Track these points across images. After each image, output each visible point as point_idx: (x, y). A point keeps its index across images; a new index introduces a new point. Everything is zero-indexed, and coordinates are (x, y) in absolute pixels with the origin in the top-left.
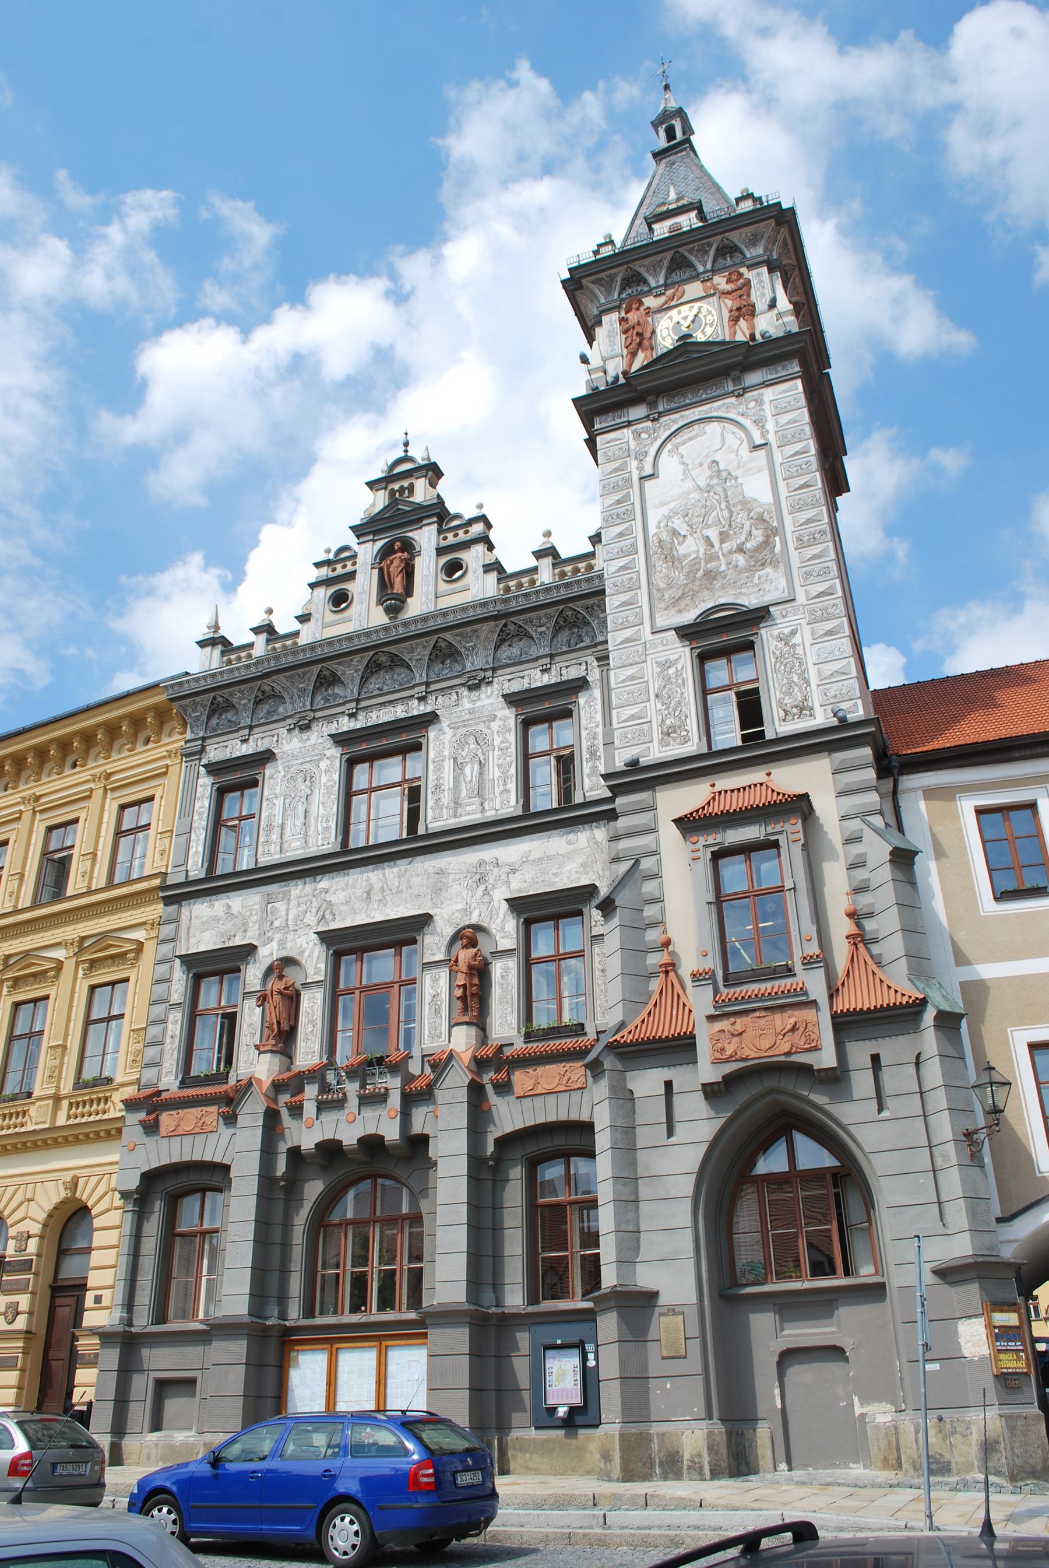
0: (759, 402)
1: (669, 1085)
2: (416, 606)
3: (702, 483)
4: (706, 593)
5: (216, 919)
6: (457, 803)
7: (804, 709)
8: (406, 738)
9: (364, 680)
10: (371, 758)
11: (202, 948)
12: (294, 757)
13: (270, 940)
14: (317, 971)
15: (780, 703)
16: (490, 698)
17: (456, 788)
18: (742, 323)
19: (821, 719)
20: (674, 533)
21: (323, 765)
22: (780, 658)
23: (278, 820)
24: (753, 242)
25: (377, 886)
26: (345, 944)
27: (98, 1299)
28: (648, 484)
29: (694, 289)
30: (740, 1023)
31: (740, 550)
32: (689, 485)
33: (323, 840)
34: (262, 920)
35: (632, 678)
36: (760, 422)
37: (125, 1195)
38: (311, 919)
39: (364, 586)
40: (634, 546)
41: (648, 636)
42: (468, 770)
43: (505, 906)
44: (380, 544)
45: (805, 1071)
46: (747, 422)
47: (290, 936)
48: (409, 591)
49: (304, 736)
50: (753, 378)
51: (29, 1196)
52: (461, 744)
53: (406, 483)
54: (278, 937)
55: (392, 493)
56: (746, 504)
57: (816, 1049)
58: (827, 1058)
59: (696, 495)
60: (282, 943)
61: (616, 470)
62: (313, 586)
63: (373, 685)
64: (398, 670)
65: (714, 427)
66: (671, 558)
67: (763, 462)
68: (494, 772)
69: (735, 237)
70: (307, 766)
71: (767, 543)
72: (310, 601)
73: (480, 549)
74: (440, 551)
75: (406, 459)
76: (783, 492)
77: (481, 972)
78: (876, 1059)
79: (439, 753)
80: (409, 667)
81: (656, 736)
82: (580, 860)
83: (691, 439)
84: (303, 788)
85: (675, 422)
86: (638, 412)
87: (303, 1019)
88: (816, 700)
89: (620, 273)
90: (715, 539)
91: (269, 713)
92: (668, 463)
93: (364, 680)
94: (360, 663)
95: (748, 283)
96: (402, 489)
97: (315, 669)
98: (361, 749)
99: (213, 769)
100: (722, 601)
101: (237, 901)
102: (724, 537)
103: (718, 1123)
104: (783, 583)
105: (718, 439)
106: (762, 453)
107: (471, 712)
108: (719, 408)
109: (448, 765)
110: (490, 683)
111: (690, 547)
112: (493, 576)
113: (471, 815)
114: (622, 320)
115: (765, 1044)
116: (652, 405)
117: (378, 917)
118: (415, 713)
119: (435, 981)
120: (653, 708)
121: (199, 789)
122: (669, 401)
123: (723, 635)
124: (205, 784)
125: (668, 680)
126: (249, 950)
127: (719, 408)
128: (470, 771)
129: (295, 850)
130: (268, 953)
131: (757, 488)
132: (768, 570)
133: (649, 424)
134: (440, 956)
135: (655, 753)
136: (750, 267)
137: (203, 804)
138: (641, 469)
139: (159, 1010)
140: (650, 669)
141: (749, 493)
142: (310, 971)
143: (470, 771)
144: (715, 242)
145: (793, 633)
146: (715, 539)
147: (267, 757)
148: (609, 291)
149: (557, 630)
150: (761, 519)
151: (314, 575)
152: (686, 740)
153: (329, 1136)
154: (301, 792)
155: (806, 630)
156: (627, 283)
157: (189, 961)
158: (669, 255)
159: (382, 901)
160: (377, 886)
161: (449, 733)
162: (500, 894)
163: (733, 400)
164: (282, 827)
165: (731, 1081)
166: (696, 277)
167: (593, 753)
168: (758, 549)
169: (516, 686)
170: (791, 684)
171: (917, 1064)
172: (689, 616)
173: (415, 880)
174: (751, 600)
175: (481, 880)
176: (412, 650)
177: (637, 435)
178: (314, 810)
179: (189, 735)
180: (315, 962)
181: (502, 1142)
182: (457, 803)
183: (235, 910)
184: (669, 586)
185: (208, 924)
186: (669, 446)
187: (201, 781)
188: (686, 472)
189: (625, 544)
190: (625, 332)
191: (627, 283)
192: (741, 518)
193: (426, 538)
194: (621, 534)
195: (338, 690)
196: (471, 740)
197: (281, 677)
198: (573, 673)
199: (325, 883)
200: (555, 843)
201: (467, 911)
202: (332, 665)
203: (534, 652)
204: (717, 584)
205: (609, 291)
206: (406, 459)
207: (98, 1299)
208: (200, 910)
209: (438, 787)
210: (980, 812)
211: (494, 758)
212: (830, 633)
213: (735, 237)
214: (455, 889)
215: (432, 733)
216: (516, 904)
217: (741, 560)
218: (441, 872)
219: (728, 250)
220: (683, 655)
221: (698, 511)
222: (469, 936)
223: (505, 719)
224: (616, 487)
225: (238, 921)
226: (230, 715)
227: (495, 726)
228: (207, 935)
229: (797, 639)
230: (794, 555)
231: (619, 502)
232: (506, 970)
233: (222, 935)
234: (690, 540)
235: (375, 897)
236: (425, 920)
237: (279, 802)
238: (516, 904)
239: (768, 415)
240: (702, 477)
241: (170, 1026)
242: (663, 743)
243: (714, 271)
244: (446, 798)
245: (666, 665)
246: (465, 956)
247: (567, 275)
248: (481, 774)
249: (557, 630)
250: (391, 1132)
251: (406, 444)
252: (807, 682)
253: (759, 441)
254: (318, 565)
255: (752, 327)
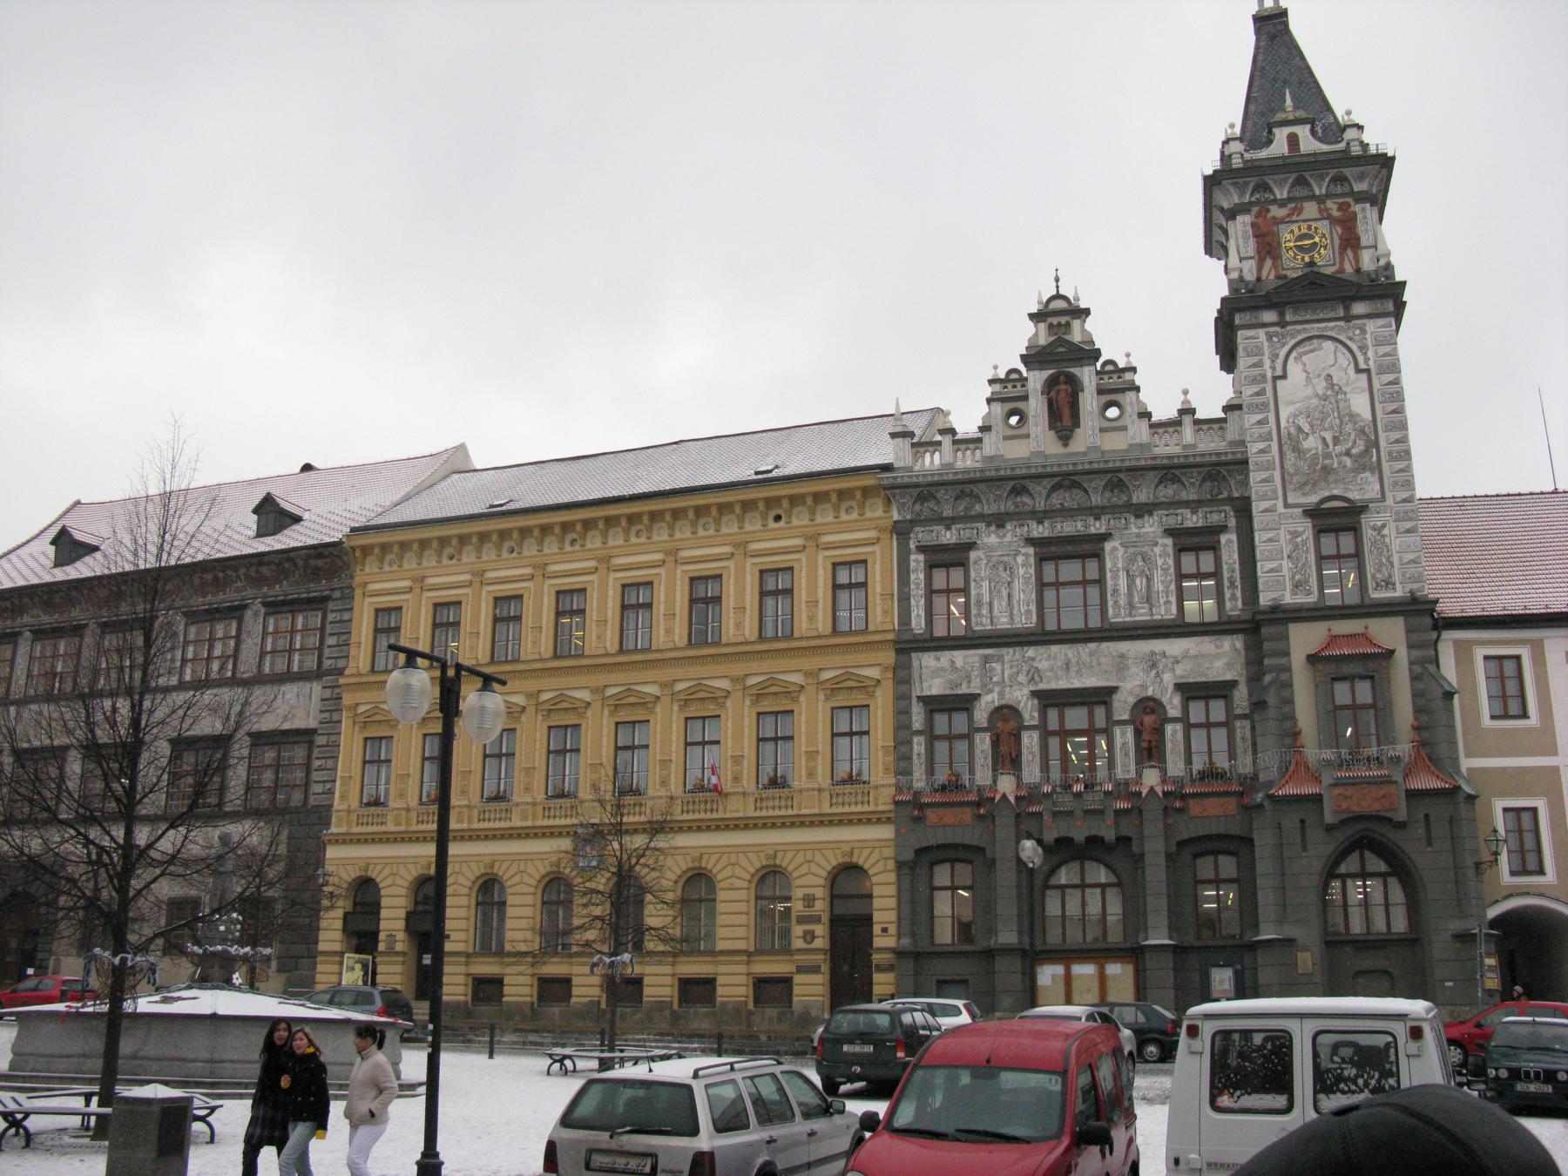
0: (1363, 331)
1: (1302, 821)
2: (1087, 438)
3: (1320, 392)
4: (1323, 484)
5: (942, 669)
6: (1131, 606)
7: (1389, 583)
8: (1090, 548)
9: (1048, 496)
10: (1056, 558)
11: (934, 692)
12: (991, 549)
13: (991, 691)
14: (1032, 718)
15: (1373, 577)
16: (1151, 526)
17: (1130, 595)
18: (1350, 253)
19: (1399, 592)
20: (1300, 429)
21: (1020, 559)
22: (1374, 544)
23: (986, 598)
24: (1361, 178)
25: (1074, 660)
26: (1049, 699)
27: (885, 930)
28: (1279, 383)
29: (1311, 209)
30: (1349, 791)
31: (1348, 453)
32: (1309, 391)
33: (1025, 619)
34: (982, 676)
35: (1270, 540)
36: (1363, 348)
37: (900, 865)
38: (1022, 678)
39: (1036, 406)
40: (1270, 433)
41: (1281, 509)
42: (1138, 582)
43: (1171, 688)
44: (1047, 373)
45: (1390, 820)
46: (1354, 347)
47: (1007, 690)
48: (1077, 424)
49: (1001, 532)
50: (1359, 308)
51: (809, 858)
52: (1132, 560)
53: (1063, 320)
54: (997, 689)
55: (1051, 326)
56: (1353, 417)
57: (1395, 810)
58: (1401, 815)
59: (1315, 401)
60: (1001, 694)
61: (1254, 365)
62: (989, 401)
63: (1056, 500)
64: (1075, 491)
65: (1328, 345)
66: (1298, 450)
67: (1365, 384)
68: (1158, 587)
69: (1347, 172)
70: (1006, 559)
71: (1367, 451)
72: (989, 414)
73: (1132, 394)
74: (1100, 392)
75: (1058, 296)
76: (1379, 415)
77: (1159, 731)
78: (1426, 816)
79: (1115, 564)
80: (1085, 491)
81: (1289, 587)
82: (1225, 660)
83: (1312, 351)
84: (1005, 575)
85: (1299, 332)
86: (1269, 316)
87: (1024, 751)
88: (1397, 578)
89: (1253, 182)
90: (1329, 441)
91: (966, 509)
92: (1294, 368)
93: (1048, 496)
94: (1048, 483)
95: (1354, 216)
96: (1059, 324)
97: (1012, 483)
98: (1048, 551)
99: (921, 549)
100: (1335, 492)
101: (959, 656)
102: (1336, 441)
103: (1332, 848)
104: (1378, 487)
105: (1332, 356)
106: (1364, 376)
107: (1138, 535)
108: (1332, 329)
109: (1122, 577)
110: (1151, 514)
111: (1311, 443)
112: (1144, 424)
113: (1142, 615)
114: (1253, 225)
115: (1365, 804)
116: (1282, 314)
117: (1077, 684)
118: (1093, 530)
119: (1123, 734)
120: (1286, 565)
121: (913, 564)
122: (1295, 313)
123: (1337, 521)
124: (917, 560)
125: (1297, 546)
126: (976, 697)
127: (1332, 329)
128: (1140, 583)
129: (1003, 623)
130: (989, 700)
131: (1360, 404)
132: (1368, 474)
133: (1277, 329)
134: (1126, 717)
135: (1288, 599)
136: (1357, 201)
137: (918, 577)
138: (1274, 369)
139: (903, 734)
140: (1283, 536)
141: (1355, 409)
142: (1026, 716)
143: (1140, 583)
144: (1332, 172)
145: (1384, 526)
146: (1329, 441)
147: (971, 546)
148: (1242, 194)
149: (1204, 480)
150: (1362, 431)
151: (988, 391)
152: (1309, 593)
153: (1063, 833)
154: (1003, 582)
155: (1392, 525)
156: (1256, 189)
157: (926, 700)
158: (1294, 176)
159: (1078, 671)
160: (1074, 660)
161: (1122, 551)
162: (1169, 679)
163: (1342, 323)
164: (991, 604)
165: (1343, 822)
166: (1313, 197)
167: (1232, 583)
168: (1361, 455)
169: (1172, 522)
170: (1381, 564)
171: (1451, 821)
172: (1313, 499)
173: (1103, 660)
174: (1354, 495)
175: (1154, 666)
176: (1091, 481)
177: (1269, 337)
178: (1016, 594)
179: (896, 517)
180: (1030, 712)
181: (1181, 844)
182: (1131, 606)
183: (959, 663)
184: (1296, 473)
185: (938, 672)
186: (1294, 354)
187: (913, 557)
188: (1308, 379)
189: (1264, 430)
190: (1255, 236)
191: (1256, 189)
192: (1348, 427)
193: (1087, 376)
194: (1260, 422)
195: (1026, 499)
196: (1139, 558)
197: (983, 486)
198: (1215, 518)
199: (1031, 652)
200: (1205, 645)
201: (1144, 687)
202: (1027, 483)
203: (1184, 496)
204: (1331, 478)
205: (1242, 194)
206: (1058, 296)
207: (885, 930)
208: (927, 662)
209: (1115, 591)
210: (1486, 658)
211: (1158, 576)
212: (1408, 531)
213: (1347, 172)
214: (1134, 670)
215: (1108, 546)
216: (1179, 687)
217: (1348, 462)
218: (1122, 656)
219: (1340, 179)
220: (1306, 528)
221: (1317, 415)
222: (1148, 706)
223: (1165, 545)
224: (1254, 381)
225: (962, 674)
226: (932, 504)
227: (1157, 550)
228: (937, 681)
229: (1385, 531)
230: (1385, 465)
231: (1257, 394)
232: (1175, 732)
233: (950, 682)
234: (1311, 438)
235: (1073, 669)
236: (1112, 690)
237: (985, 584)
238: (1179, 687)
239: (1369, 343)
240: (1321, 386)
241: (916, 748)
242: (1294, 593)
243: (1328, 196)
244: (1122, 601)
245: (1295, 534)
246: (1148, 720)
247: (1210, 172)
248: (1149, 587)
249: (1204, 480)
250: (1109, 834)
251: (1057, 280)
252: (1392, 564)
253: (1362, 366)
254: (991, 382)
255: (1357, 259)
